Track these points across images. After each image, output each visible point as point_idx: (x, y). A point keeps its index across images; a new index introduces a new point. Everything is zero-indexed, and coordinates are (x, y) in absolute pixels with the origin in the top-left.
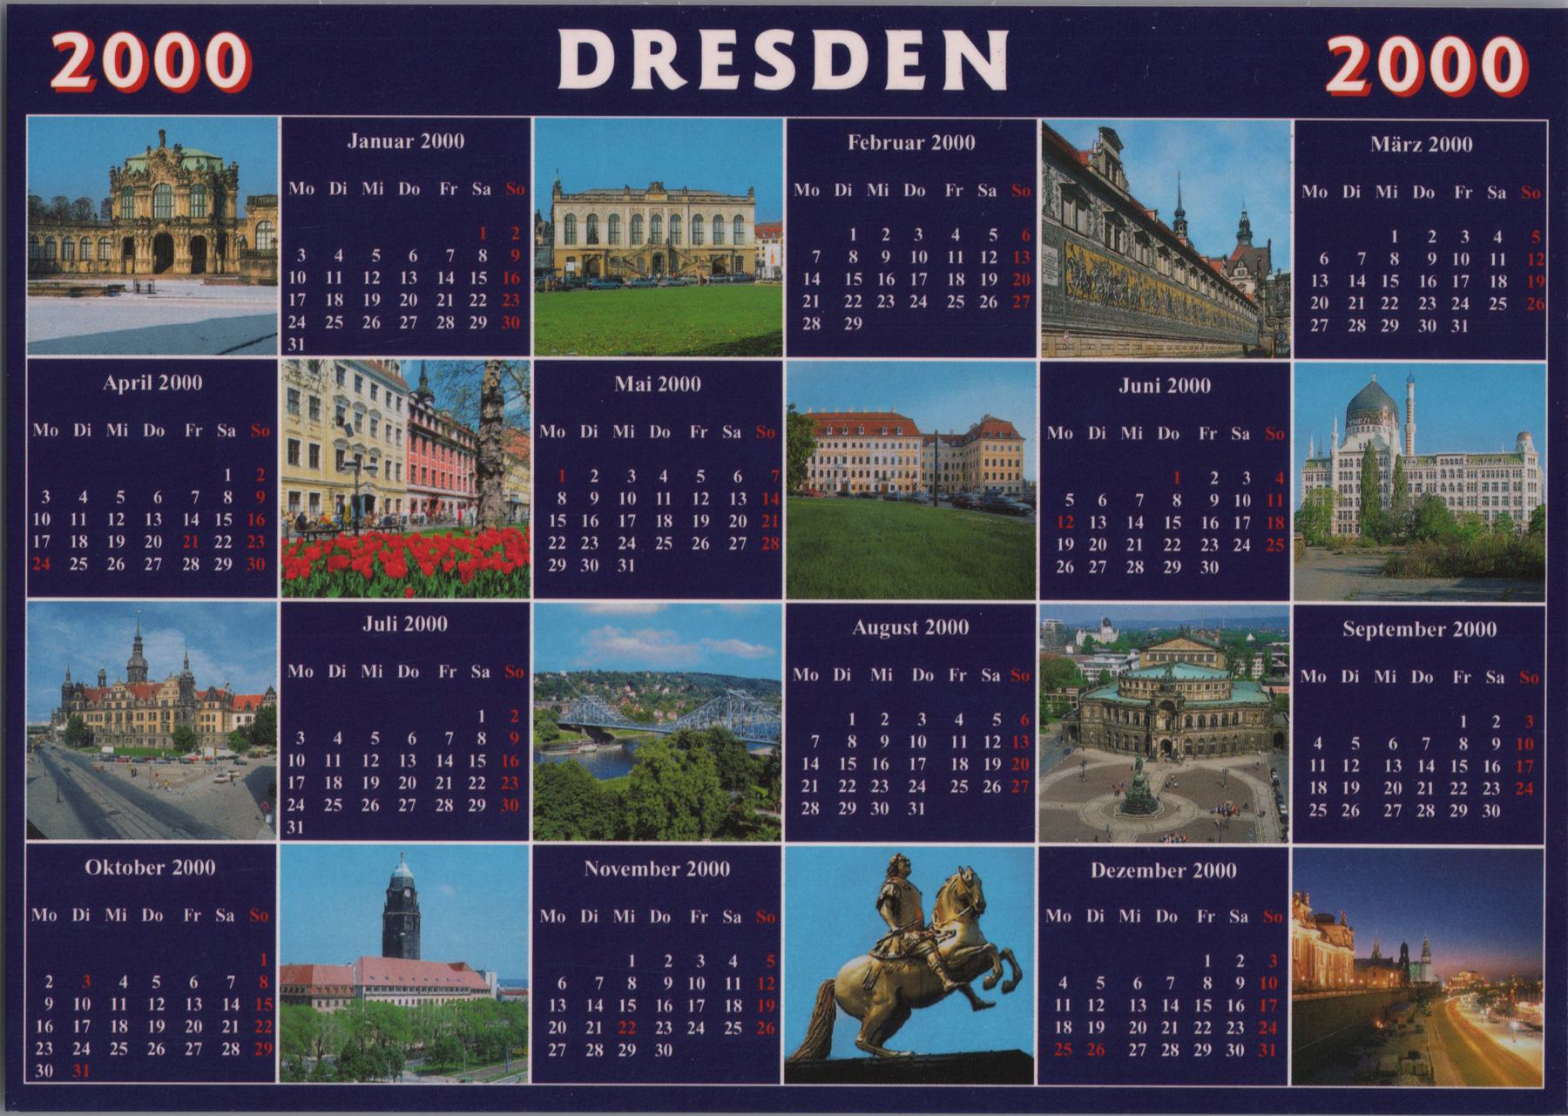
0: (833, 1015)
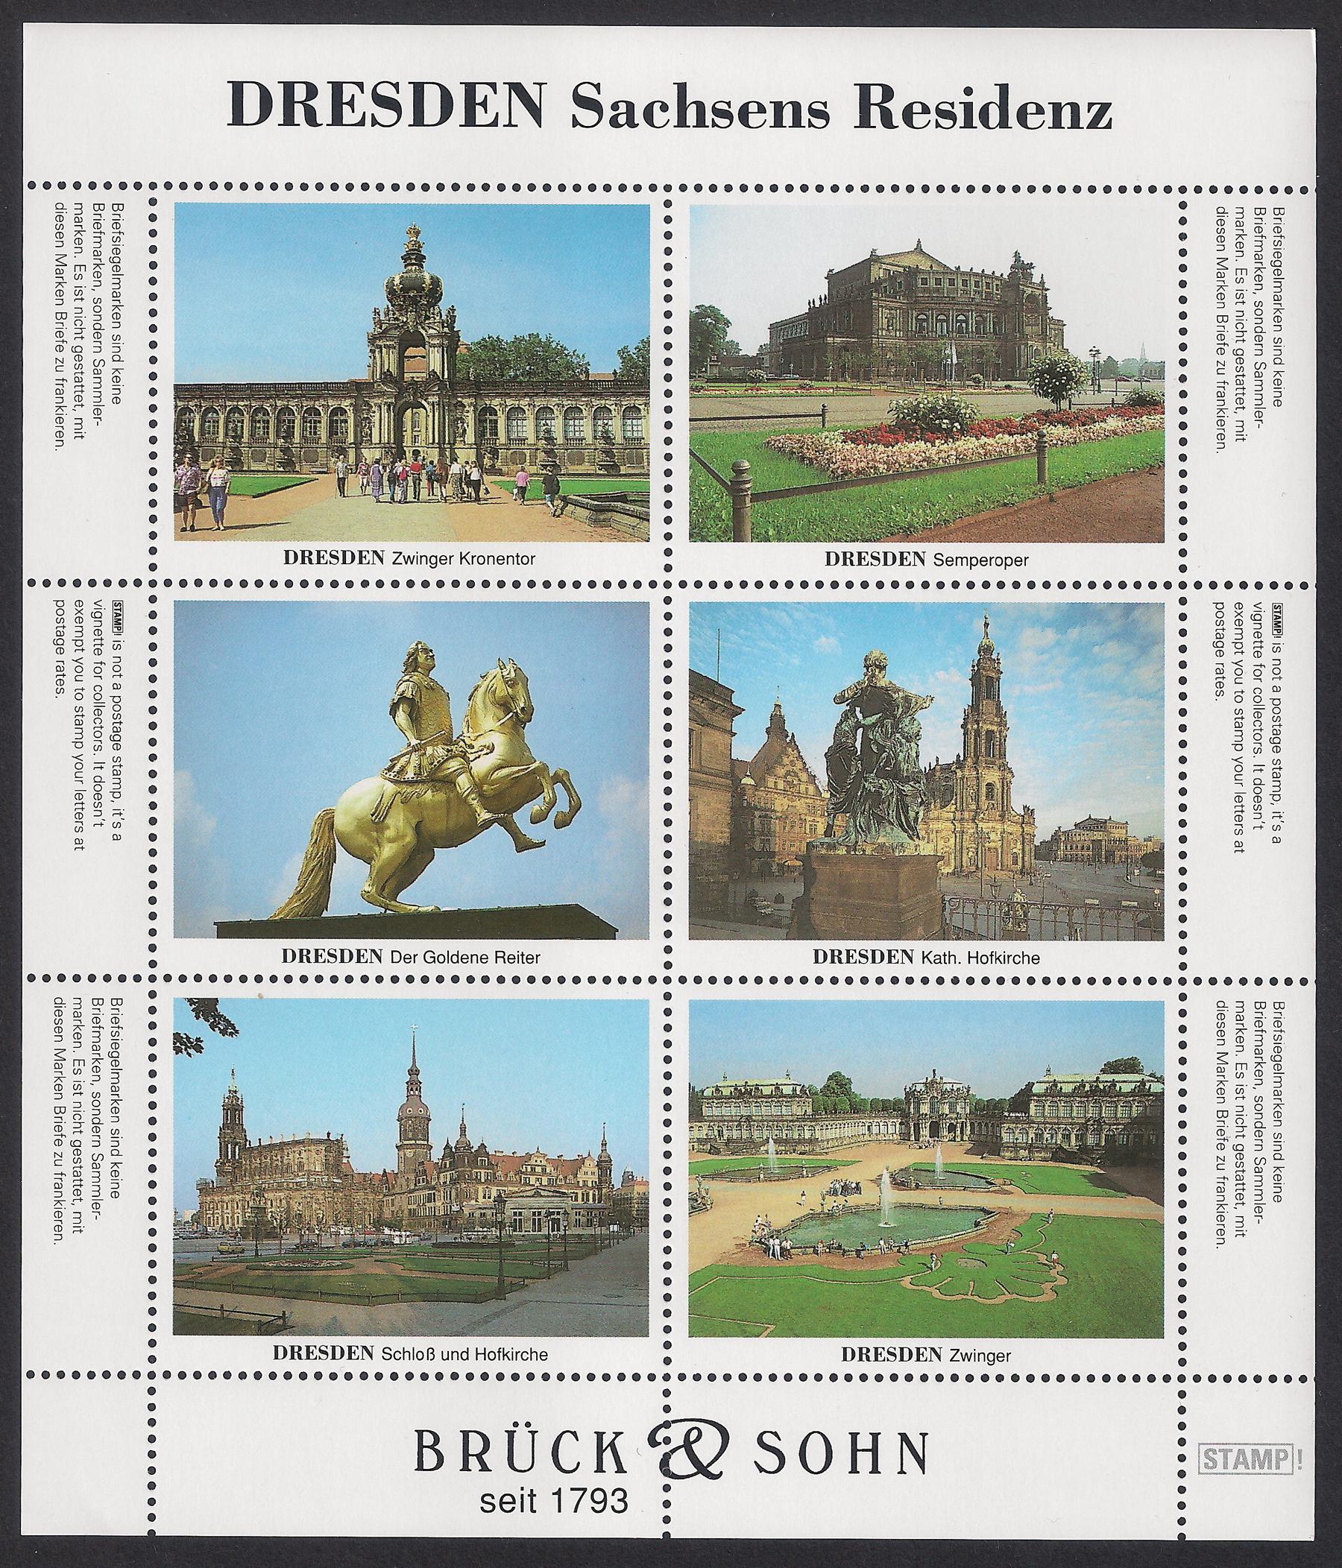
0: (331, 858)
